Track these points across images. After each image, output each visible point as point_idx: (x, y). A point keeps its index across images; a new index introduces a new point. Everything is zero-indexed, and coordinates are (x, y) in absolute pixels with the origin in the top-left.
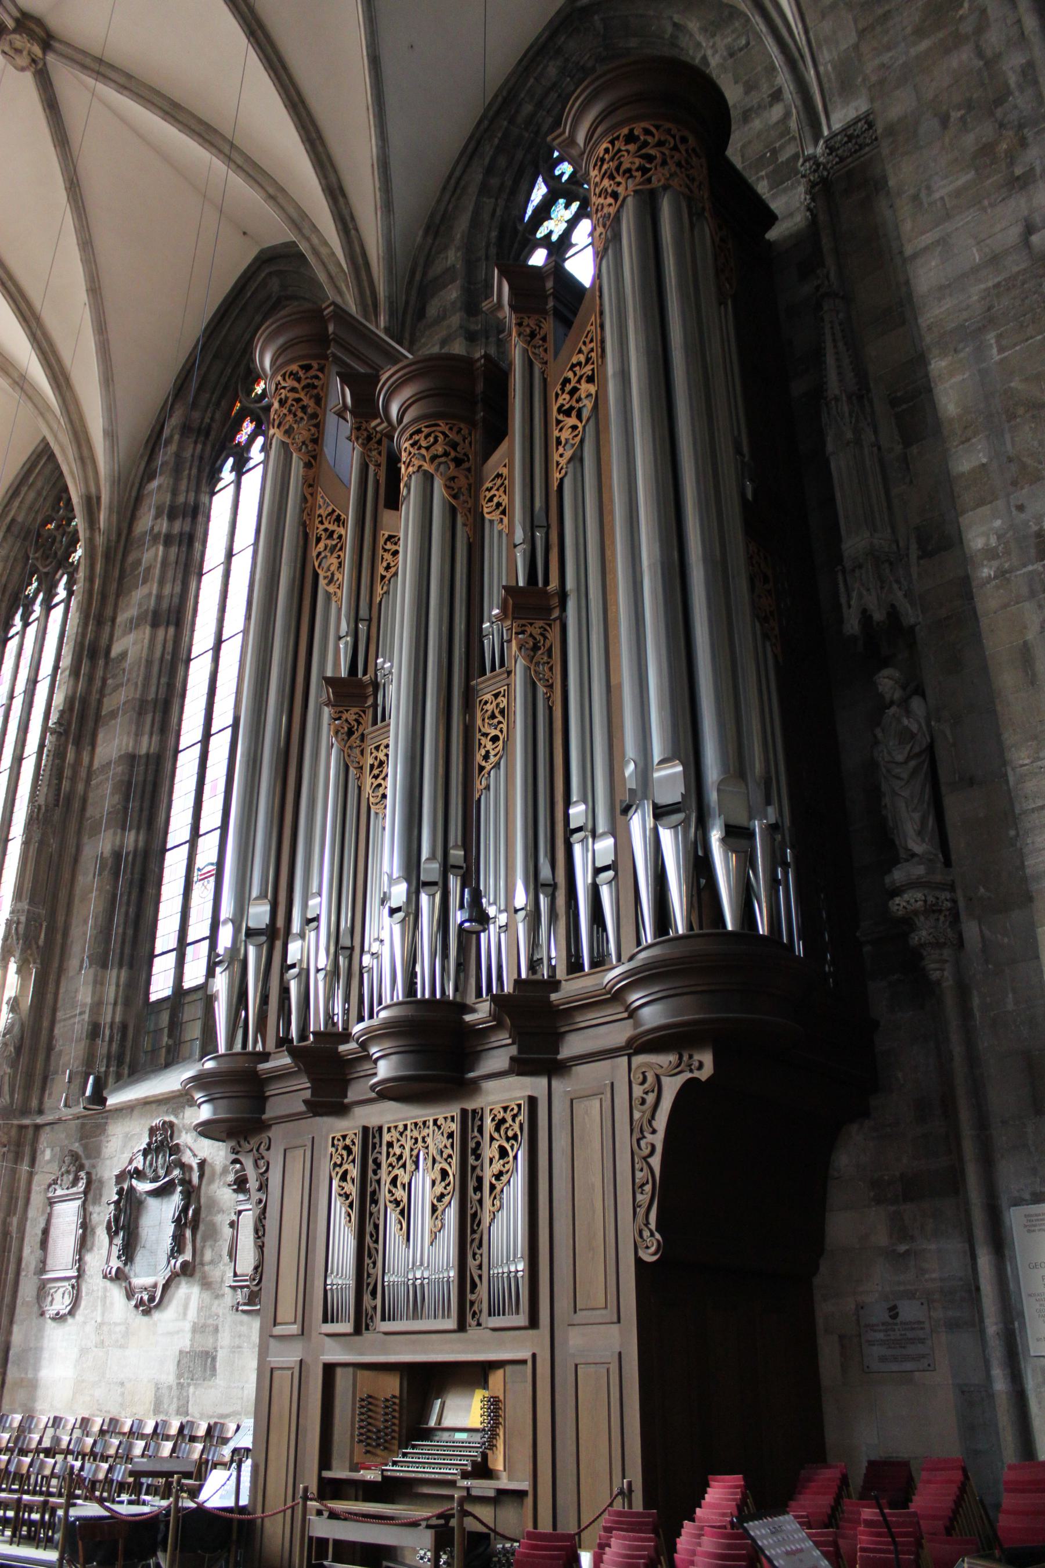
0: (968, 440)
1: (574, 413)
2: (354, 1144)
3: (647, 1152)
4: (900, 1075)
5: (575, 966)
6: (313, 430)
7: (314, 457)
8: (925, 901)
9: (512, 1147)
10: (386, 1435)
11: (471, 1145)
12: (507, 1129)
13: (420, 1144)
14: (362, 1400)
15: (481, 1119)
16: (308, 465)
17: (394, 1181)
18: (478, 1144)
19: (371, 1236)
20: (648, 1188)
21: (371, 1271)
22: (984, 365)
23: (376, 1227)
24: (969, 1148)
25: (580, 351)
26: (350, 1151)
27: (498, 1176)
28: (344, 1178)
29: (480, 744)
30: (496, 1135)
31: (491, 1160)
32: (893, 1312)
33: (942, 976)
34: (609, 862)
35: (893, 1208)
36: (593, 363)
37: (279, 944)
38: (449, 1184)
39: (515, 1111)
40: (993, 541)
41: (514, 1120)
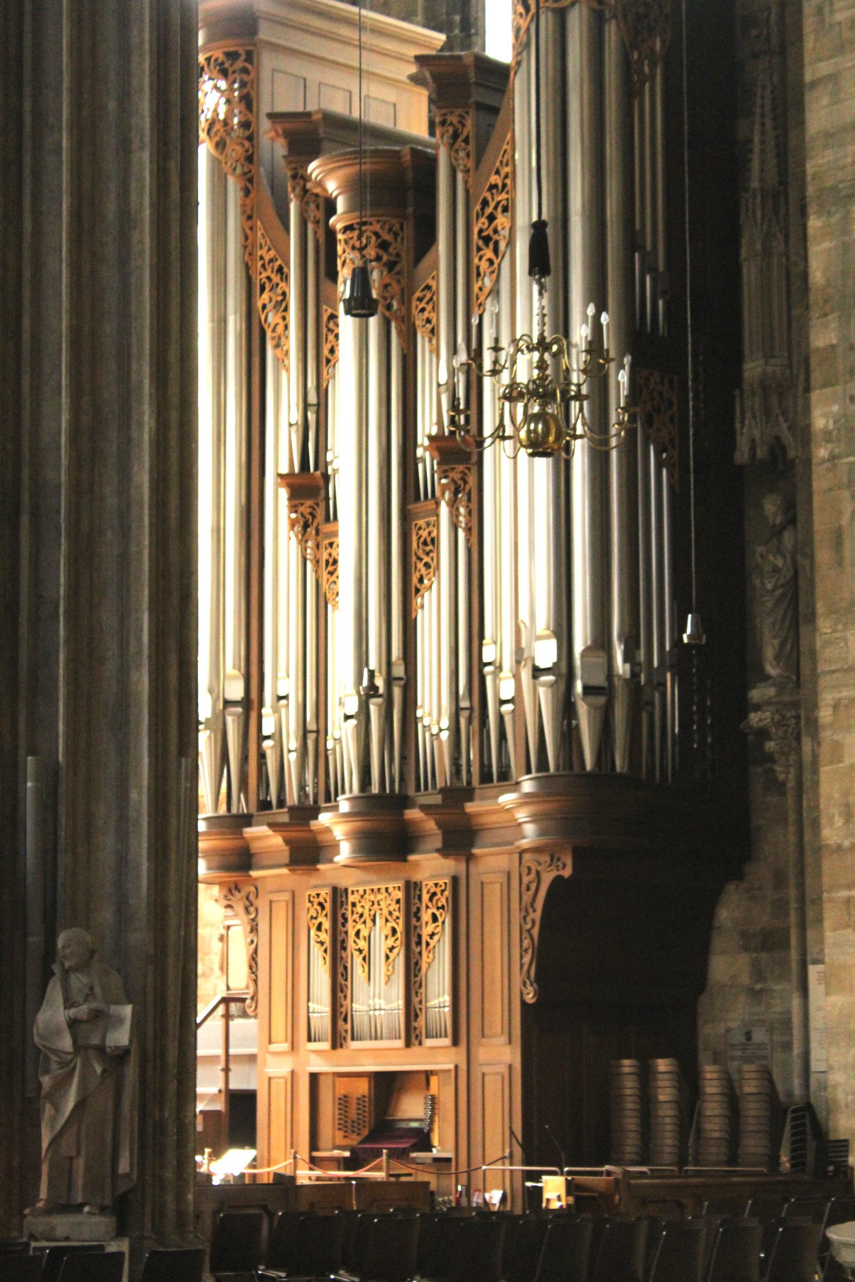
0: (825, 315)
1: (491, 245)
2: (326, 901)
3: (529, 926)
4: (766, 848)
5: (486, 777)
6: (247, 144)
7: (250, 180)
8: (772, 719)
9: (441, 915)
10: (359, 1124)
11: (414, 909)
12: (438, 900)
13: (376, 906)
14: (340, 1099)
15: (420, 890)
16: (247, 192)
17: (358, 934)
18: (418, 909)
19: (342, 975)
20: (530, 951)
21: (344, 1003)
22: (847, 238)
23: (346, 968)
24: (793, 918)
25: (498, 172)
26: (323, 908)
27: (432, 935)
28: (319, 928)
29: (416, 567)
30: (430, 904)
31: (427, 923)
32: (748, 1035)
33: (787, 778)
34: (510, 698)
35: (755, 955)
36: (507, 193)
37: (254, 715)
38: (397, 939)
39: (443, 888)
40: (831, 426)
41: (442, 894)
